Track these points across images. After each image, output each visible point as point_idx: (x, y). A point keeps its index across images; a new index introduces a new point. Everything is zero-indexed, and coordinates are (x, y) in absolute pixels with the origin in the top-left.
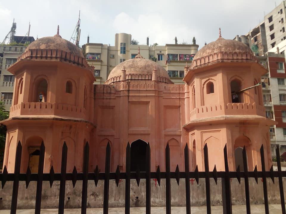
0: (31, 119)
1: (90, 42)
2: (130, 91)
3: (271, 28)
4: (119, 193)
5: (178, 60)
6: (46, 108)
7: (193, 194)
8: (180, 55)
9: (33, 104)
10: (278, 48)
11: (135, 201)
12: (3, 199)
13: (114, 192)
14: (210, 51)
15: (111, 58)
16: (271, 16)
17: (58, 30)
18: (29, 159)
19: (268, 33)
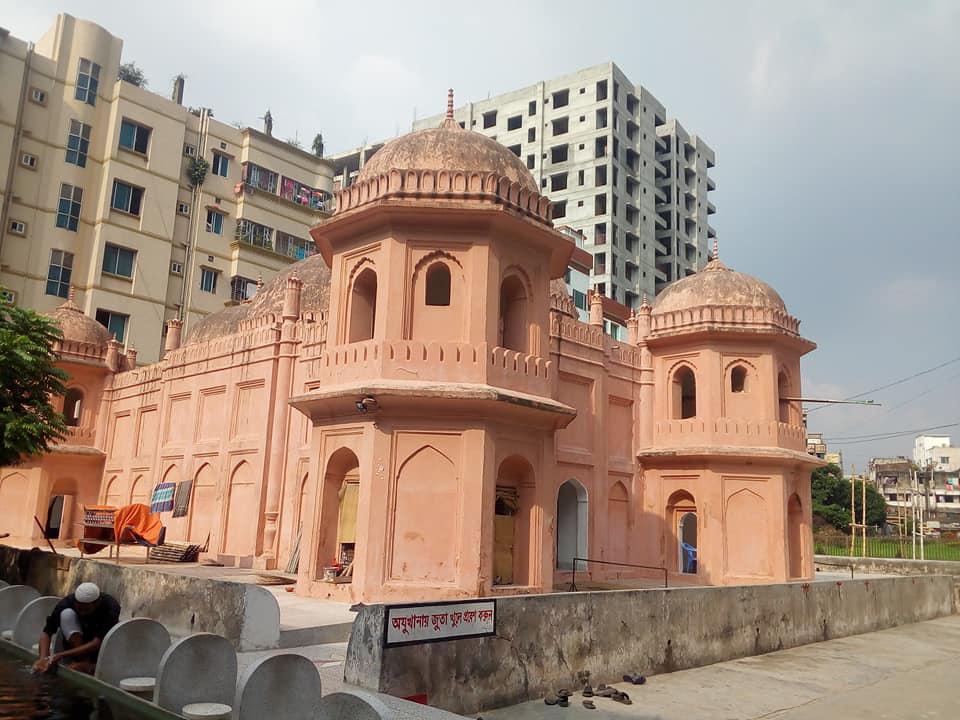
5: (278, 193)
8: (283, 178)
14: (744, 297)
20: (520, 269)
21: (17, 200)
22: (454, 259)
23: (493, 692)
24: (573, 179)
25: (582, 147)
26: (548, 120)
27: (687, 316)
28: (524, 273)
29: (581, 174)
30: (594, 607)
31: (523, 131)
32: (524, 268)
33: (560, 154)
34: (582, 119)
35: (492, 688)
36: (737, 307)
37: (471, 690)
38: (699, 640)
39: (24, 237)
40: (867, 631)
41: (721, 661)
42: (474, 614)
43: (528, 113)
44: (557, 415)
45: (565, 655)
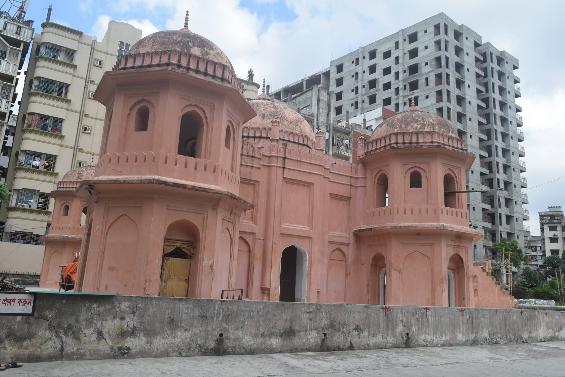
0: (189, 189)
1: (51, 21)
2: (286, 160)
3: (339, 82)
4: (388, 326)
6: (205, 170)
7: (463, 329)
9: (182, 158)
10: (365, 120)
11: (405, 339)
12: (224, 336)
13: (382, 325)
14: (419, 126)
15: (94, 65)
16: (341, 63)
17: (187, 19)
18: (162, 265)
19: (333, 88)
20: (196, 106)
21: (86, 115)
22: (150, 102)
23: (27, 352)
24: (422, 82)
25: (426, 64)
26: (406, 51)
27: (383, 141)
28: (201, 109)
29: (427, 79)
30: (140, 305)
31: (393, 58)
32: (201, 106)
33: (414, 69)
34: (426, 48)
35: (26, 348)
36: (412, 133)
37: (5, 348)
38: (256, 336)
39: (90, 134)
40: (458, 345)
41: (280, 352)
42: (13, 301)
43: (394, 48)
44: (219, 195)
45: (106, 335)
